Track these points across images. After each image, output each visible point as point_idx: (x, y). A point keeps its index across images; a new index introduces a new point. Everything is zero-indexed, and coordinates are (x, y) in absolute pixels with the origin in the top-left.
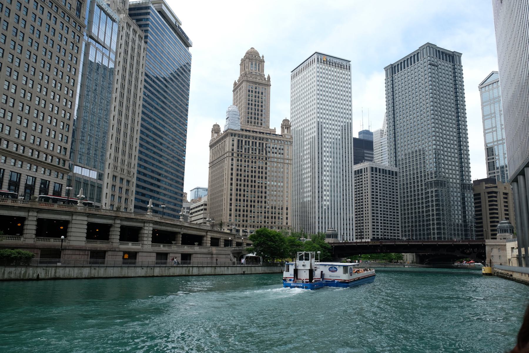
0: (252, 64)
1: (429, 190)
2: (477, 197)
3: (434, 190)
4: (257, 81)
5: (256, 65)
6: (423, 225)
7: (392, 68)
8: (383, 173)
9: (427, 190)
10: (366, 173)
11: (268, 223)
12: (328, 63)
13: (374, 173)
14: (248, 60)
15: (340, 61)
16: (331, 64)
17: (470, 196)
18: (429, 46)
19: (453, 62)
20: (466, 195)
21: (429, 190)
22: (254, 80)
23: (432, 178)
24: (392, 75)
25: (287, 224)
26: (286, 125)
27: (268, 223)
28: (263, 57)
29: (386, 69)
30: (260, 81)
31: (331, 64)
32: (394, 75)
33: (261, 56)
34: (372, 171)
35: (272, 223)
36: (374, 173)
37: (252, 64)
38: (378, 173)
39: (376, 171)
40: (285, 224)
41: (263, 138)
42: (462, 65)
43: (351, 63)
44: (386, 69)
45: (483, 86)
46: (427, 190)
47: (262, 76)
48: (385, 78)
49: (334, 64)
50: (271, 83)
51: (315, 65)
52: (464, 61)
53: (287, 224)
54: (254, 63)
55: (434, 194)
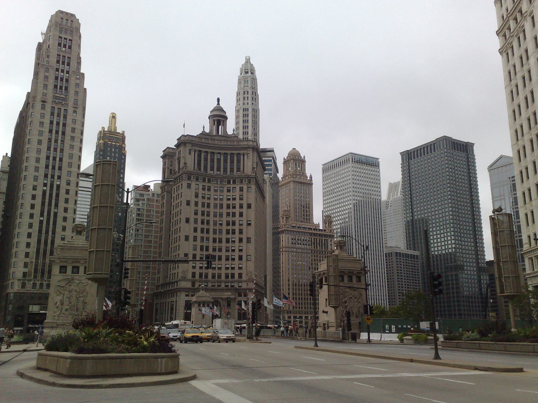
0: (296, 164)
1: (450, 274)
2: (492, 277)
3: (454, 273)
4: (302, 181)
5: (299, 165)
6: (444, 306)
8: (406, 257)
9: (447, 274)
10: (390, 258)
13: (398, 257)
14: (292, 161)
17: (485, 278)
18: (446, 139)
19: (467, 152)
20: (482, 277)
21: (450, 274)
22: (300, 180)
23: (451, 262)
24: (409, 160)
26: (328, 220)
28: (304, 157)
29: (402, 154)
32: (410, 161)
34: (397, 256)
36: (398, 257)
37: (296, 164)
38: (402, 258)
39: (400, 256)
42: (475, 153)
44: (402, 154)
45: (491, 168)
46: (447, 274)
47: (304, 174)
51: (350, 164)
52: (477, 151)
54: (297, 164)
55: (454, 278)
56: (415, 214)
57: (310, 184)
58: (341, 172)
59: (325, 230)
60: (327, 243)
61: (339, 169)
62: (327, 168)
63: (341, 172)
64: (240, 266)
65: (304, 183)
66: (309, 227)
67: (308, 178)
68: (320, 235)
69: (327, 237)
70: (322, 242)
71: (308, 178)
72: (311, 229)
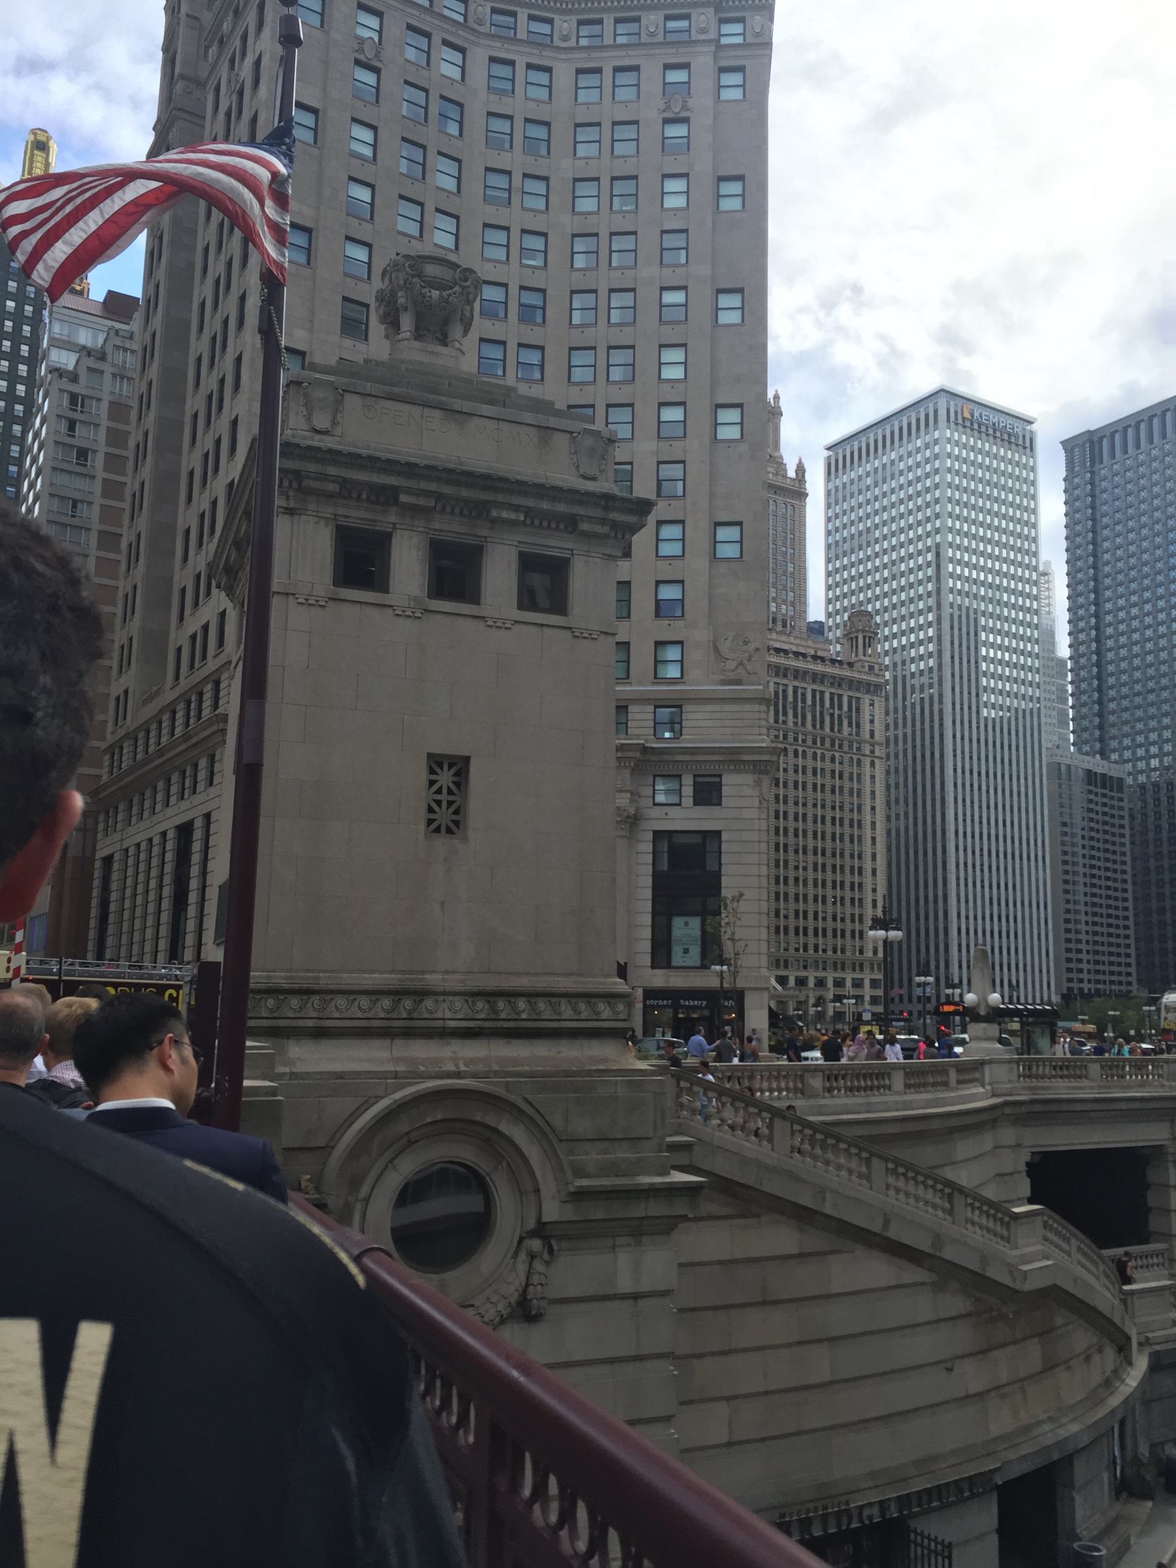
7: (1092, 442)
11: (824, 951)
12: (976, 426)
15: (1010, 421)
16: (983, 429)
25: (875, 952)
27: (824, 951)
28: (777, 397)
30: (779, 482)
31: (983, 429)
33: (770, 395)
35: (835, 951)
40: (870, 954)
41: (806, 673)
43: (1034, 427)
48: (1064, 474)
49: (991, 431)
50: (809, 487)
53: (875, 952)
56: (1110, 643)
57: (797, 492)
58: (902, 466)
59: (851, 665)
60: (858, 710)
61: (893, 455)
62: (845, 455)
63: (902, 466)
64: (669, 593)
65: (777, 489)
66: (794, 649)
67: (791, 473)
68: (837, 682)
69: (858, 690)
70: (840, 707)
71: (791, 473)
72: (804, 655)
